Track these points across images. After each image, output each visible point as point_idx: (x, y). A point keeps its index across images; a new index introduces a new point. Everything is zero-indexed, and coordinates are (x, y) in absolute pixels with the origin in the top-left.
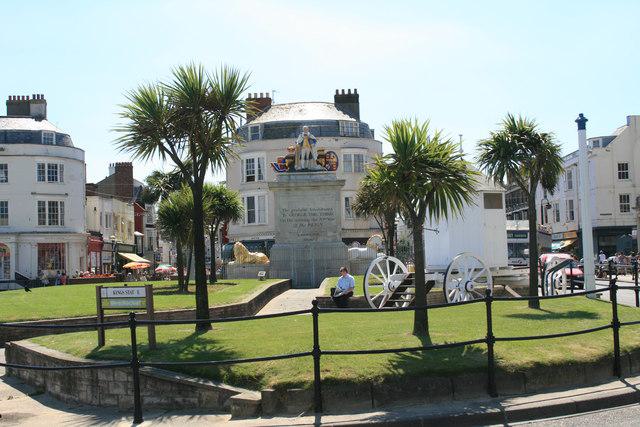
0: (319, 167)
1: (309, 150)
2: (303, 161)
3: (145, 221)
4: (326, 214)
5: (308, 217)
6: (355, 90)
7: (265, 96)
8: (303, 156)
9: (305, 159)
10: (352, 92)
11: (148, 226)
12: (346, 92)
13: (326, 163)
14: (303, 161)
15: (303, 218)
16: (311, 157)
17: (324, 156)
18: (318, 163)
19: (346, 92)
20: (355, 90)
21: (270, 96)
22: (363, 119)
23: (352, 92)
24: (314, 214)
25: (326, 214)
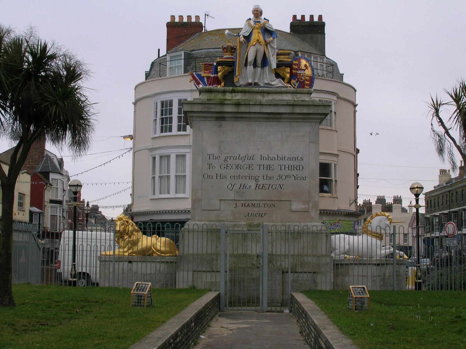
0: (277, 83)
1: (262, 49)
2: (250, 68)
3: (48, 195)
4: (291, 168)
5: (256, 172)
6: (320, 17)
7: (193, 20)
8: (251, 58)
9: (255, 65)
10: (316, 19)
11: (52, 201)
12: (307, 19)
13: (293, 76)
14: (250, 68)
15: (246, 173)
16: (265, 62)
17: (290, 65)
18: (278, 76)
19: (307, 19)
20: (320, 17)
21: (202, 20)
22: (330, 52)
23: (316, 19)
24: (269, 167)
25: (291, 168)
